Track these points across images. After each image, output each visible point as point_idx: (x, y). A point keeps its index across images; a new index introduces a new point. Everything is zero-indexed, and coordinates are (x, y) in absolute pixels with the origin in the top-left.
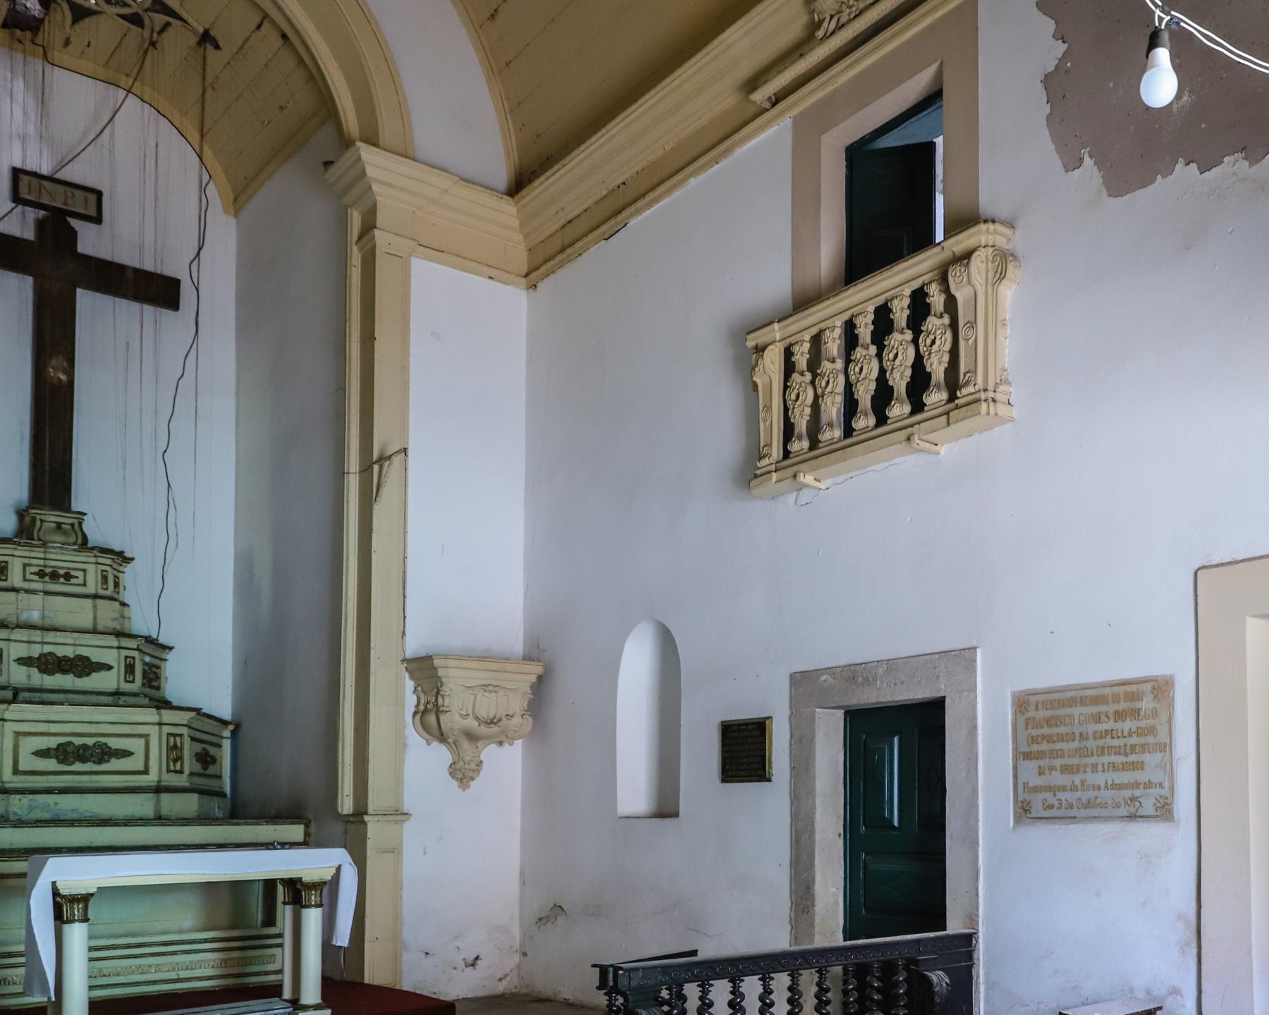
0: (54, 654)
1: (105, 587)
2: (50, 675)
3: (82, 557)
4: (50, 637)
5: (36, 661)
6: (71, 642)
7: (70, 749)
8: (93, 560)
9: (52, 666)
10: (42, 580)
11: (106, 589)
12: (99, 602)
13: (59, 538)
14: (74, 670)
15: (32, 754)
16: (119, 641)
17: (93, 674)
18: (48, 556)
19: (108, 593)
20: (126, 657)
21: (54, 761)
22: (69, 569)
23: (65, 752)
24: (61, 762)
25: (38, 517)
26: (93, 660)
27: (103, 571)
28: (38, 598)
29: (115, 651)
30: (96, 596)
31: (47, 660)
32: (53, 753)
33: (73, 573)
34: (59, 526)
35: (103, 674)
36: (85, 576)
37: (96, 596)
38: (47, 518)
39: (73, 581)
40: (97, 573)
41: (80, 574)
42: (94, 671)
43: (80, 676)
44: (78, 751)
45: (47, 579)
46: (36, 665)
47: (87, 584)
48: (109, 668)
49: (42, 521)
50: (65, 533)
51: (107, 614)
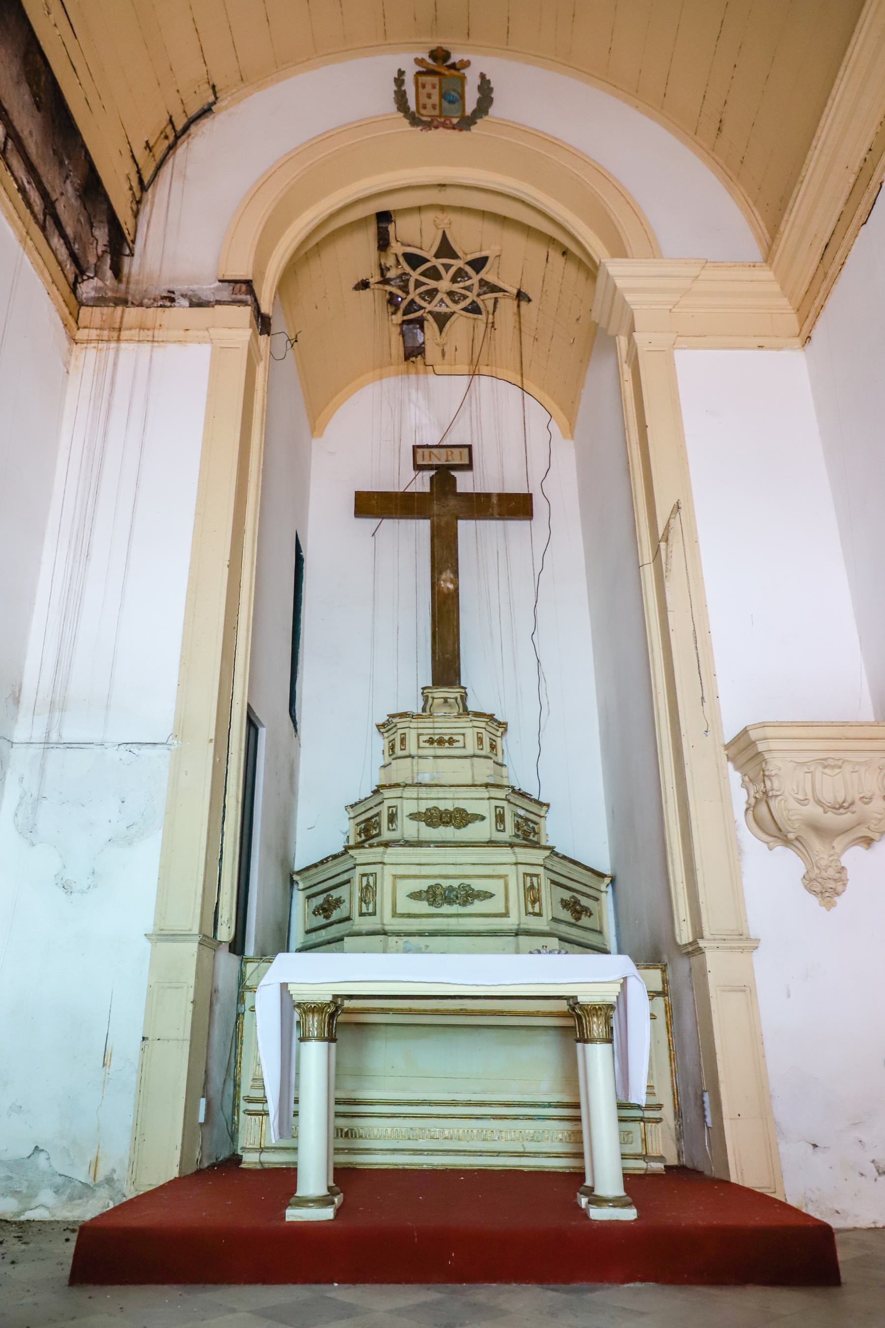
0: (437, 808)
1: (481, 747)
2: (434, 828)
3: (463, 722)
4: (434, 792)
5: (423, 815)
6: (451, 796)
8: (470, 724)
9: (436, 820)
10: (431, 746)
11: (482, 749)
12: (475, 759)
13: (447, 710)
14: (453, 822)
15: (407, 896)
16: (488, 791)
17: (470, 824)
18: (436, 725)
19: (483, 753)
20: (496, 807)
21: (426, 903)
22: (452, 734)
23: (435, 895)
24: (432, 904)
25: (430, 695)
26: (469, 812)
27: (478, 733)
29: (487, 801)
30: (474, 756)
31: (432, 814)
32: (424, 895)
33: (455, 738)
34: (446, 700)
35: (478, 824)
36: (464, 740)
37: (474, 756)
38: (436, 695)
39: (455, 745)
40: (473, 734)
41: (460, 738)
42: (470, 822)
43: (459, 828)
44: (445, 892)
45: (435, 744)
46: (423, 819)
47: (466, 746)
48: (483, 818)
49: (433, 698)
50: (450, 706)
51: (484, 771)
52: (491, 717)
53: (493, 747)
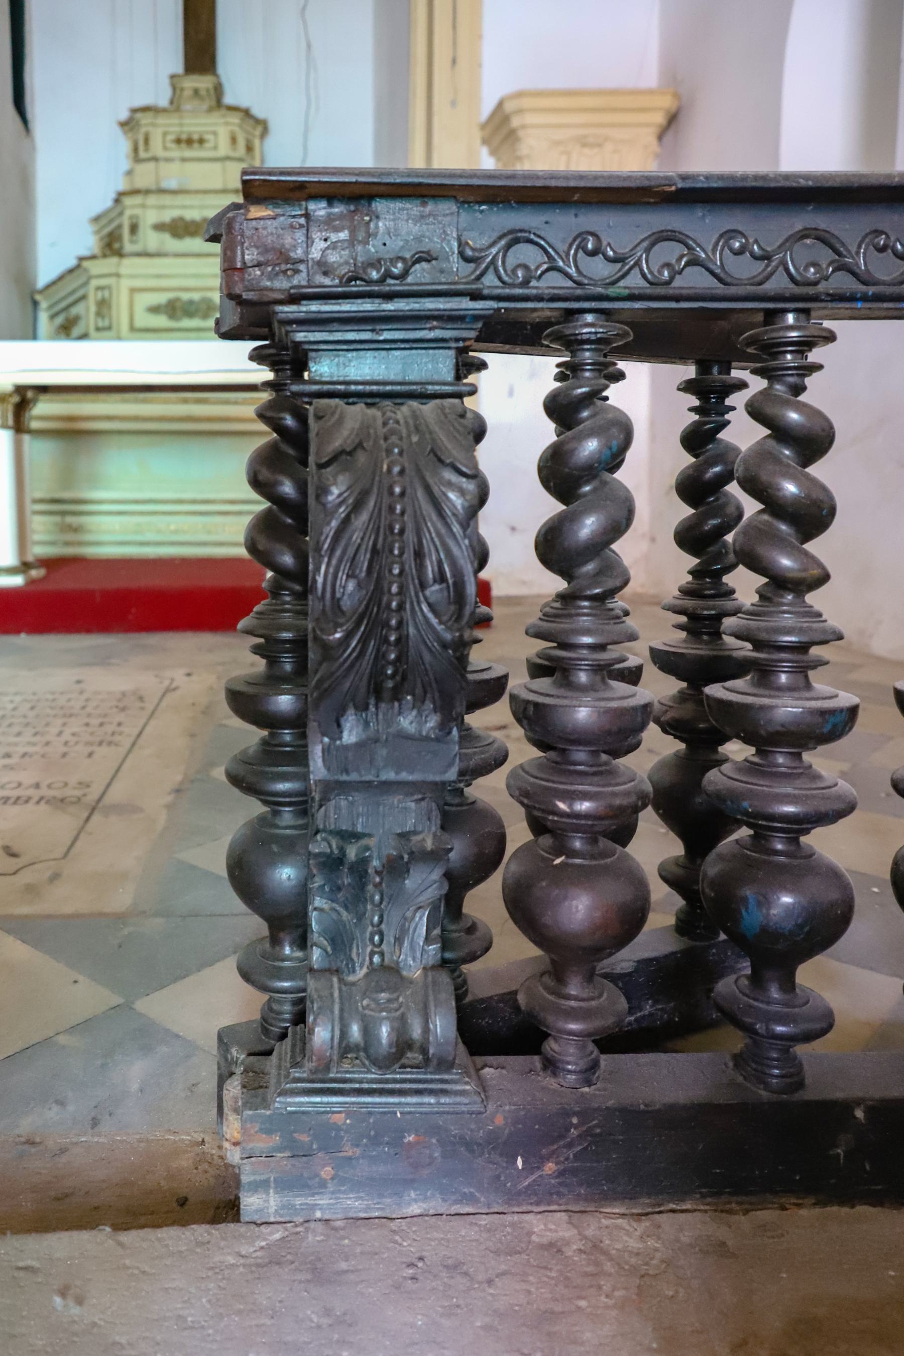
7: (178, 304)
8: (222, 121)
28: (176, 166)
39: (207, 145)
52: (246, 113)
53: (249, 149)
